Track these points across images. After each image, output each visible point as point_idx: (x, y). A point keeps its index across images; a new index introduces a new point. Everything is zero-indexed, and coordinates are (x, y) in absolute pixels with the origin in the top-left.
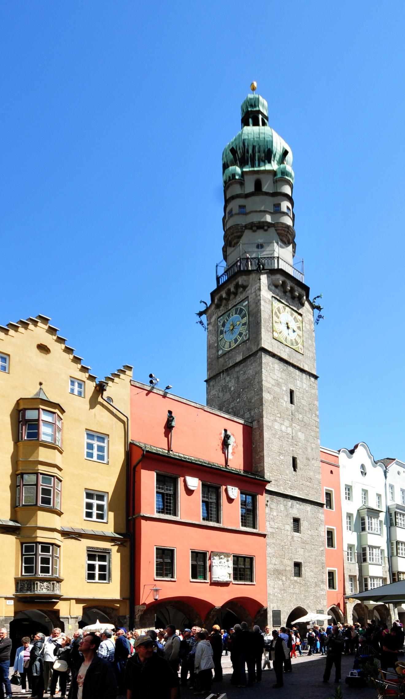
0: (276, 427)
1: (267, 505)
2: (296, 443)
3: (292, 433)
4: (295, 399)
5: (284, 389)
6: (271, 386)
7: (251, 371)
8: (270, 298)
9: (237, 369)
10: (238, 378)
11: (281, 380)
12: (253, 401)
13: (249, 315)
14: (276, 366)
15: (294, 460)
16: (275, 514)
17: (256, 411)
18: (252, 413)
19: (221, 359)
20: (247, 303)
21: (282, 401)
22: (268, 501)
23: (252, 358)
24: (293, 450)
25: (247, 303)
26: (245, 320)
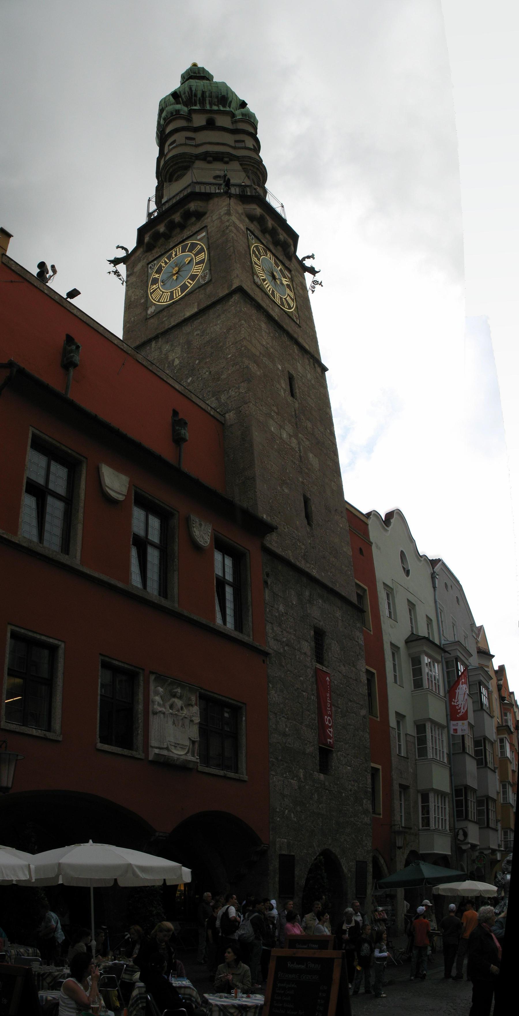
0: (272, 429)
1: (266, 583)
2: (306, 471)
3: (300, 450)
4: (297, 391)
5: (280, 367)
6: (258, 354)
7: (217, 328)
8: (244, 229)
9: (187, 329)
10: (189, 343)
11: (272, 351)
12: (223, 377)
13: (208, 249)
14: (263, 325)
15: (306, 501)
16: (282, 608)
17: (232, 393)
18: (223, 398)
19: (152, 321)
20: (204, 234)
21: (278, 386)
22: (268, 575)
23: (219, 307)
24: (303, 483)
25: (204, 234)
26: (202, 256)
